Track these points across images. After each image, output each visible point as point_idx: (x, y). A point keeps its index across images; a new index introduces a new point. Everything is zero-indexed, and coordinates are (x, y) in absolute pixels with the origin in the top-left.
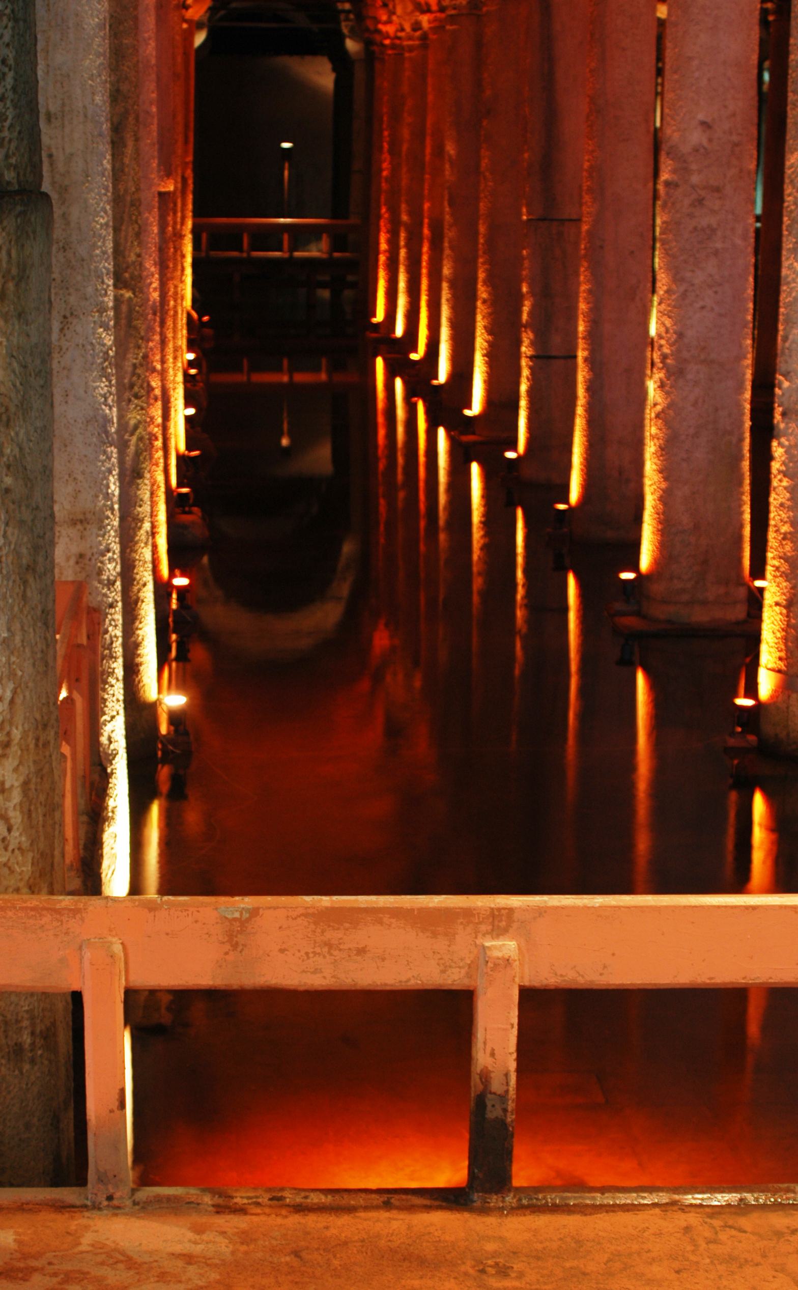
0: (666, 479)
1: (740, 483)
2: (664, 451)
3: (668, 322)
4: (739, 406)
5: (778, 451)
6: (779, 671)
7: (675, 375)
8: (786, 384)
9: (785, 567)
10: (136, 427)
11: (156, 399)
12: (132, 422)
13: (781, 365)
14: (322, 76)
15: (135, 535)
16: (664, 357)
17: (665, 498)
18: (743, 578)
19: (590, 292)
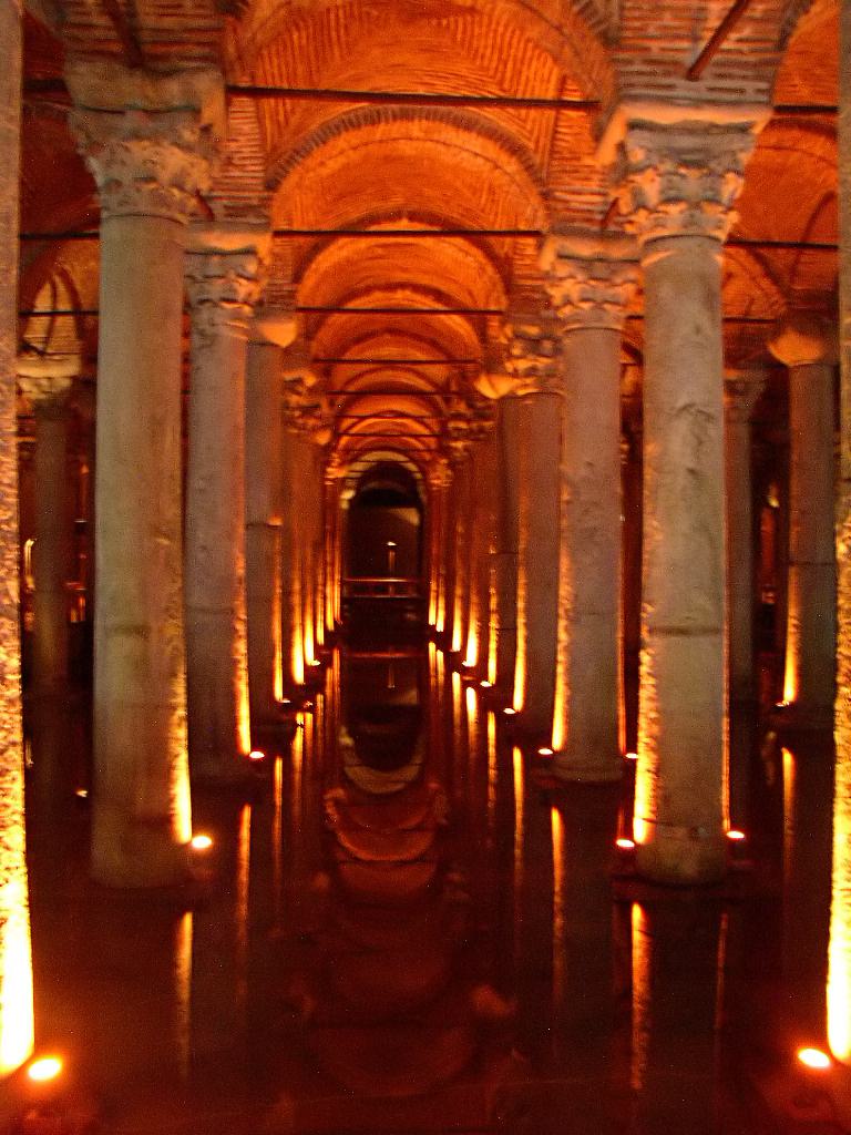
0: (570, 688)
1: (616, 691)
2: (569, 671)
3: (568, 588)
4: (614, 642)
5: (645, 657)
6: (649, 821)
7: (573, 620)
8: (650, 609)
9: (653, 743)
10: (170, 640)
11: (240, 637)
12: (168, 636)
13: (645, 595)
14: (412, 517)
15: (168, 719)
16: (566, 611)
17: (569, 701)
18: (618, 749)
19: (526, 584)
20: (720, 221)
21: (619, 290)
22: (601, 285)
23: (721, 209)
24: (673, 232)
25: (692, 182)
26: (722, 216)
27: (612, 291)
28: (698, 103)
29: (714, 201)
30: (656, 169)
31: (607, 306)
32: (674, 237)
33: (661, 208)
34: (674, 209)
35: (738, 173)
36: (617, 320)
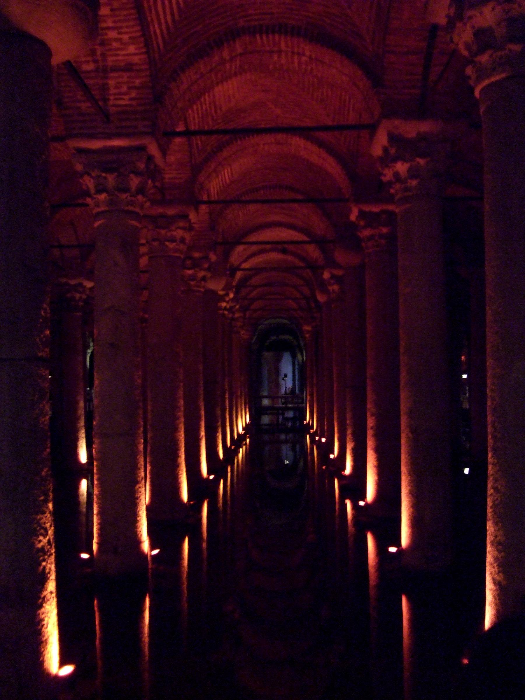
20: (132, 201)
21: (174, 233)
22: (163, 232)
23: (128, 194)
24: (103, 209)
25: (111, 180)
26: (133, 198)
27: (169, 234)
28: (109, 136)
29: (126, 190)
30: (89, 174)
31: (167, 243)
32: (103, 212)
33: (95, 196)
34: (103, 197)
35: (138, 174)
36: (176, 250)
